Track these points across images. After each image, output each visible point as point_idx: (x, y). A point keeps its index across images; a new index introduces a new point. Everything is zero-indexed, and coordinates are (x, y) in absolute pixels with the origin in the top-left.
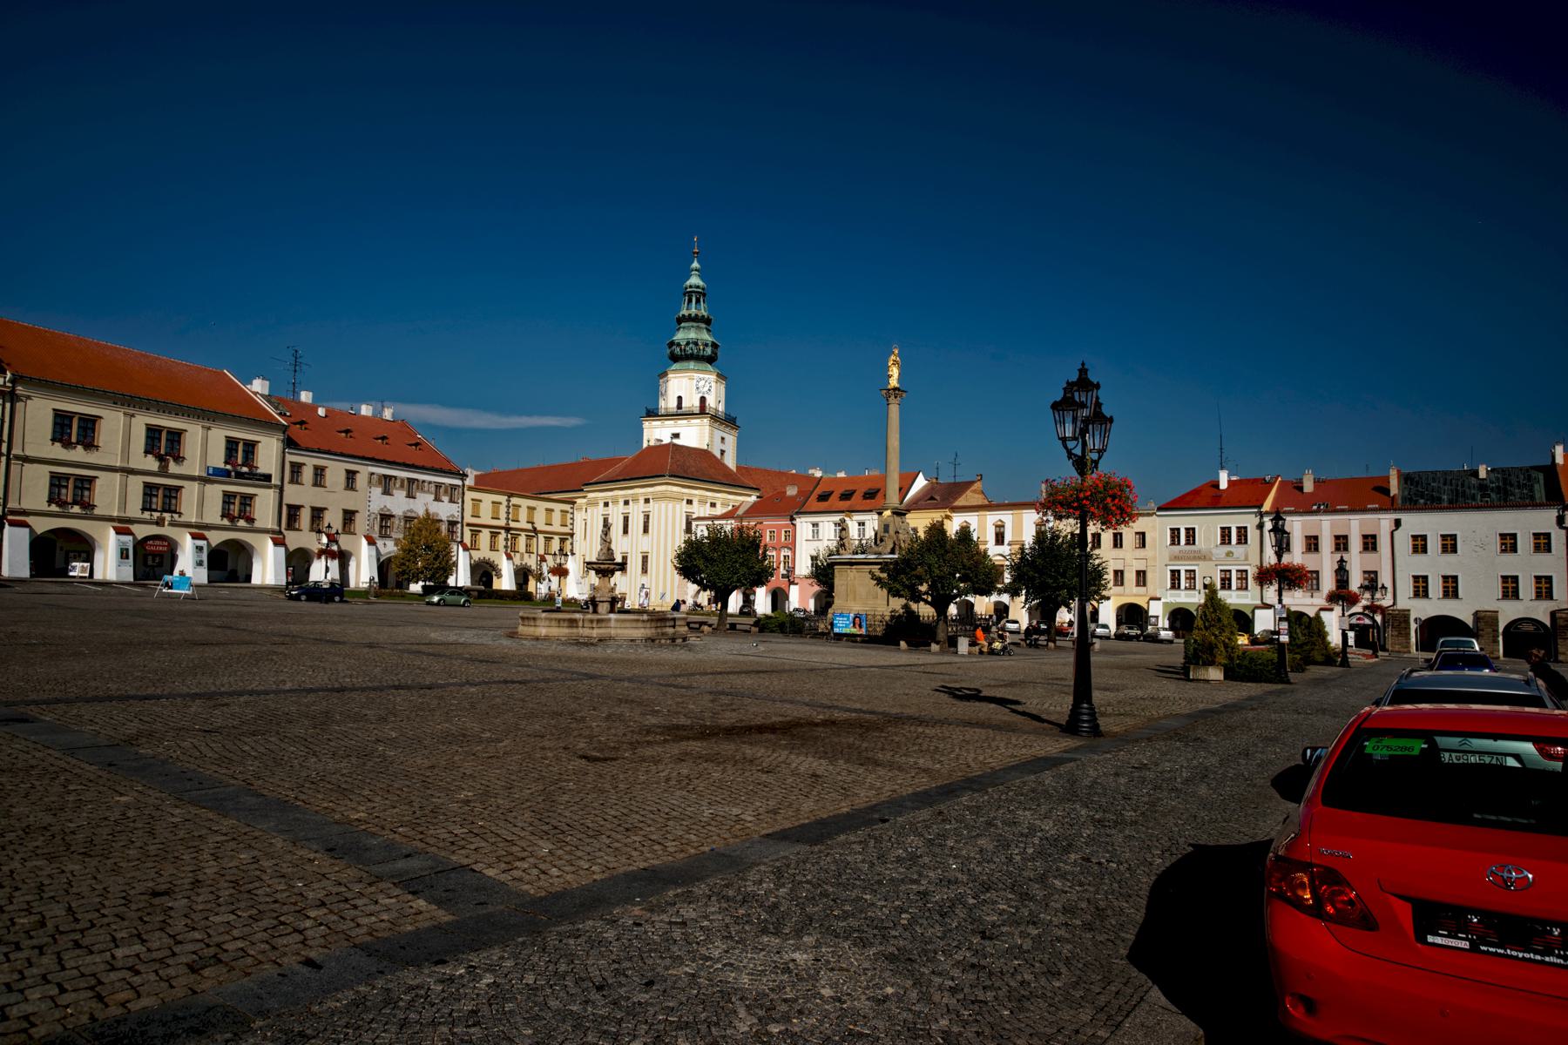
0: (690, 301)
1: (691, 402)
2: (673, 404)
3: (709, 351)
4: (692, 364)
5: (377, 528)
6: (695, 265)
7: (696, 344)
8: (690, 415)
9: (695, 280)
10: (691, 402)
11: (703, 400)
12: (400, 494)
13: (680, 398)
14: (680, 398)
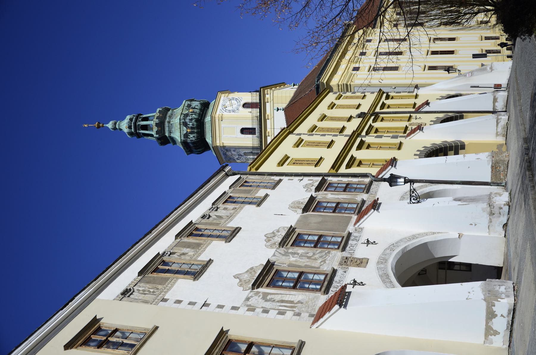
0: (145, 127)
1: (249, 118)
2: (250, 141)
3: (195, 104)
4: (208, 119)
5: (297, 296)
6: (110, 125)
7: (186, 115)
8: (262, 119)
9: (124, 125)
10: (249, 118)
11: (245, 105)
12: (214, 249)
13: (244, 131)
14: (244, 131)
